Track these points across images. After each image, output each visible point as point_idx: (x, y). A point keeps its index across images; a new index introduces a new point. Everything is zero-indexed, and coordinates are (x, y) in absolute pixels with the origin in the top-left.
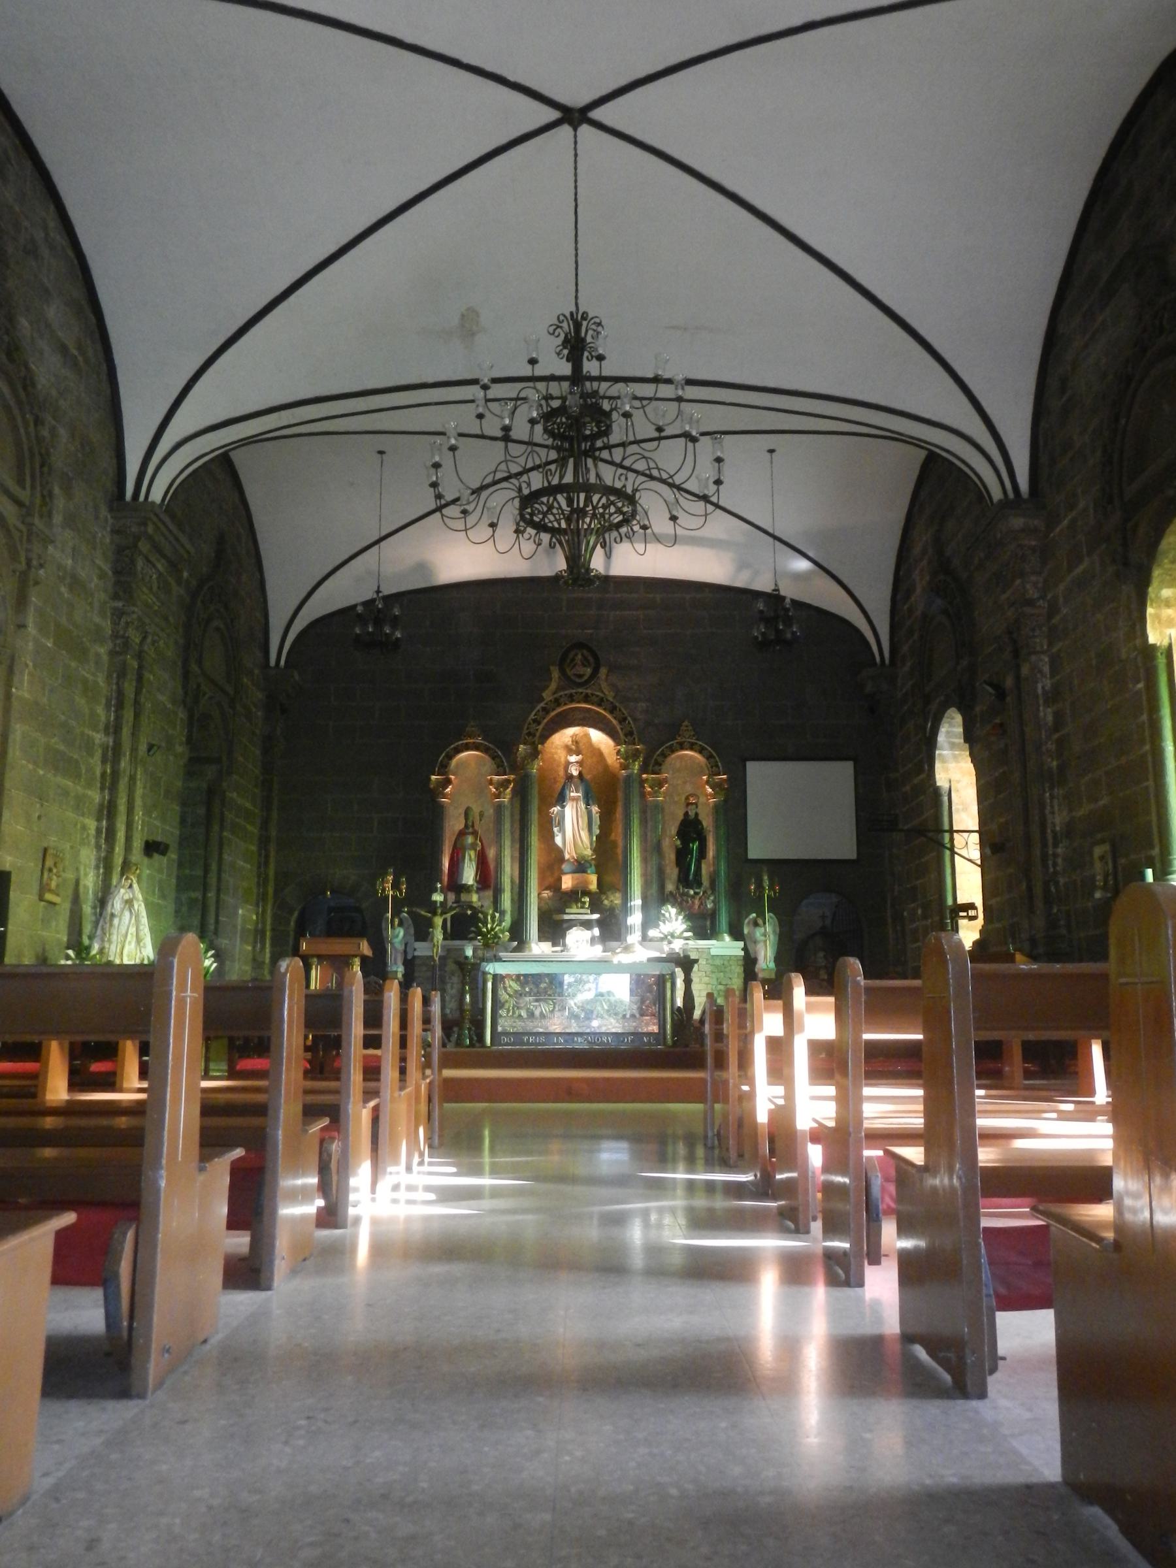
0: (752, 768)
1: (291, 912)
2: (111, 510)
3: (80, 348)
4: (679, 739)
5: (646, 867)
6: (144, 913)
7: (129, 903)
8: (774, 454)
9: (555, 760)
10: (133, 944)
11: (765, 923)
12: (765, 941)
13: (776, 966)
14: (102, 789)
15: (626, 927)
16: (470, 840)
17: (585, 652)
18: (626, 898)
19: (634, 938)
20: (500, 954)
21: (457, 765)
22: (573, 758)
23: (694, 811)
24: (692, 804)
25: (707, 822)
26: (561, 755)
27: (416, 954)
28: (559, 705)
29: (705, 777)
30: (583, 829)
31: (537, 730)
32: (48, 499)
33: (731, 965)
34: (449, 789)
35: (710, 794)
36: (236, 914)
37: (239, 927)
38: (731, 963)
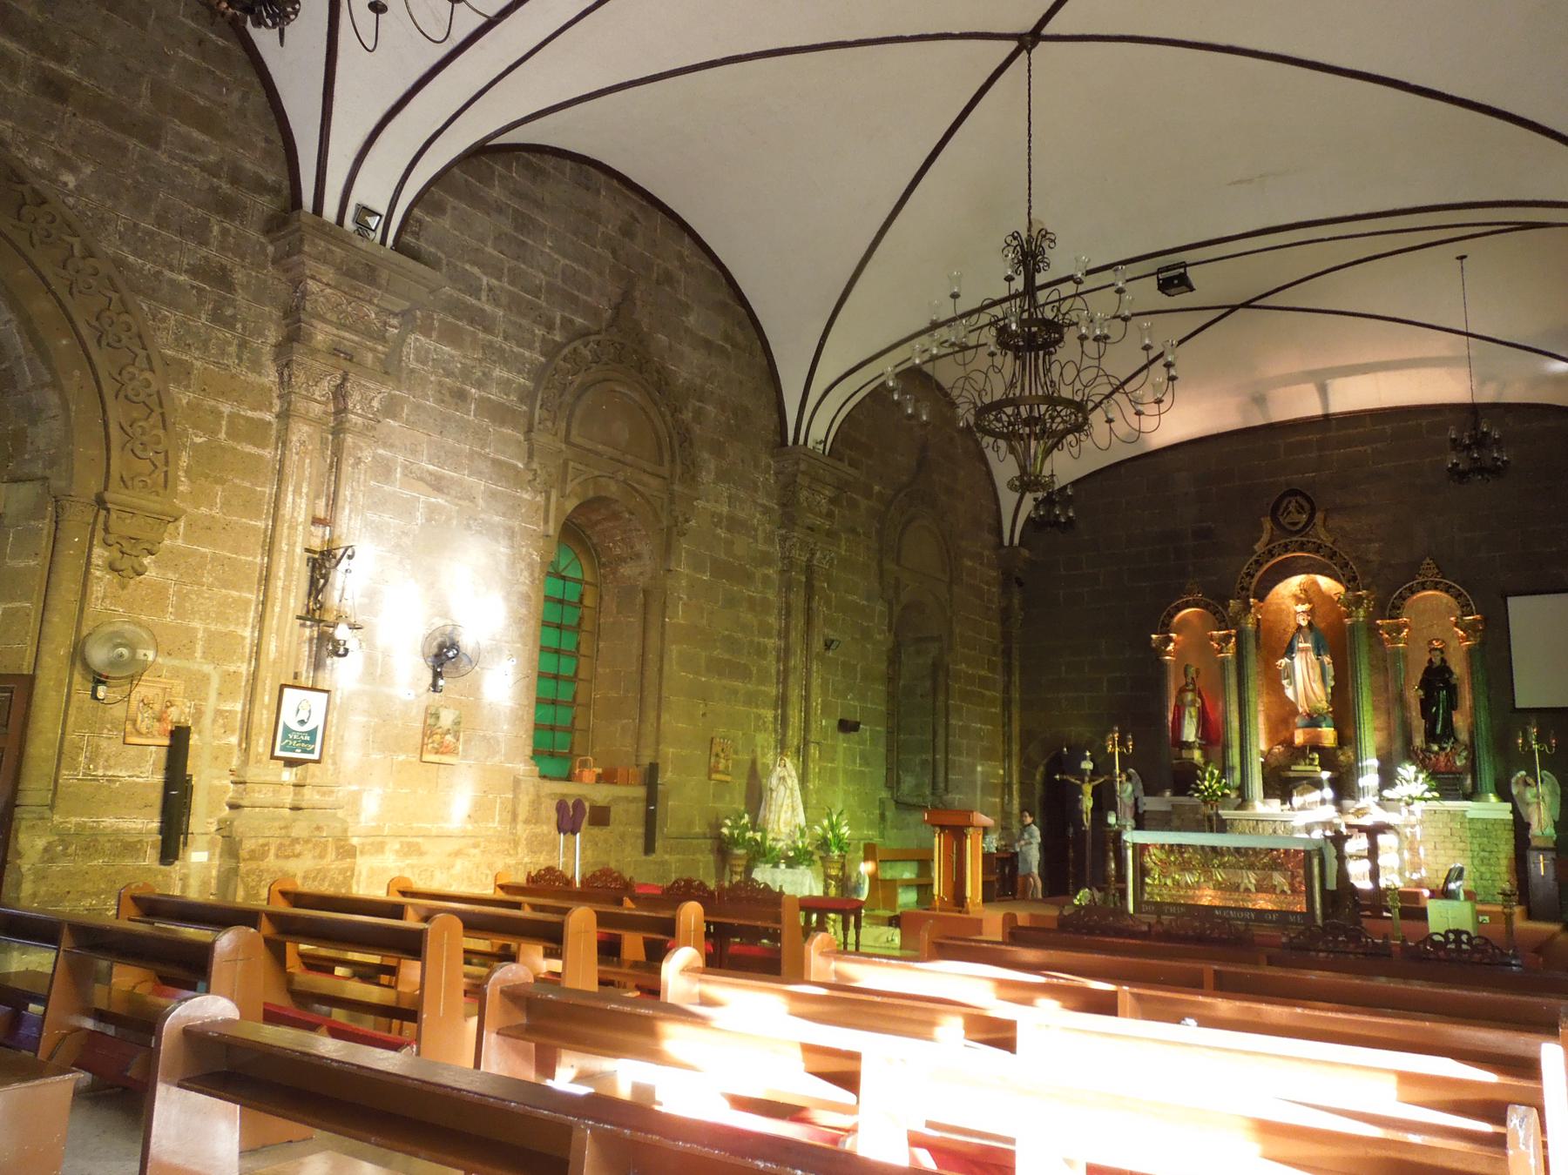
0: (1518, 607)
1: (1036, 767)
2: (773, 456)
3: (727, 338)
4: (1421, 579)
5: (1389, 718)
6: (797, 787)
7: (782, 779)
8: (1464, 260)
9: (1282, 610)
10: (790, 813)
11: (1536, 782)
12: (1539, 804)
13: (1556, 832)
14: (778, 683)
15: (1359, 788)
16: (1190, 696)
17: (1298, 498)
18: (1358, 758)
19: (1368, 801)
20: (1220, 812)
21: (1179, 622)
22: (1301, 608)
23: (1439, 658)
24: (1436, 649)
25: (1458, 667)
26: (1290, 603)
27: (1145, 808)
29: (1452, 619)
32: (691, 468)
33: (1496, 830)
34: (1169, 648)
35: (1462, 637)
36: (973, 771)
37: (979, 783)
38: (1496, 826)
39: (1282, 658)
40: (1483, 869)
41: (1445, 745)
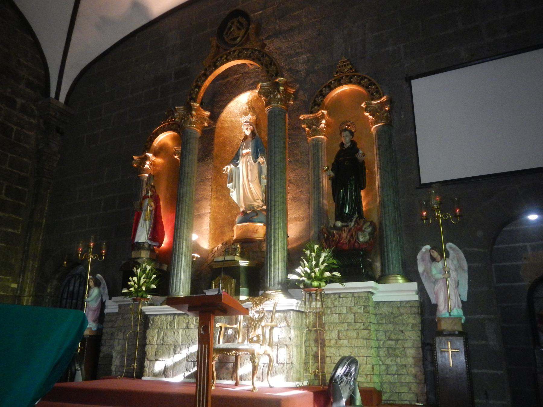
5: (309, 208)
9: (235, 127)
13: (465, 314)
23: (348, 139)
28: (216, 67)
30: (251, 182)
31: (198, 93)
33: (402, 314)
34: (147, 166)
39: (229, 164)
40: (388, 361)
41: (350, 223)
